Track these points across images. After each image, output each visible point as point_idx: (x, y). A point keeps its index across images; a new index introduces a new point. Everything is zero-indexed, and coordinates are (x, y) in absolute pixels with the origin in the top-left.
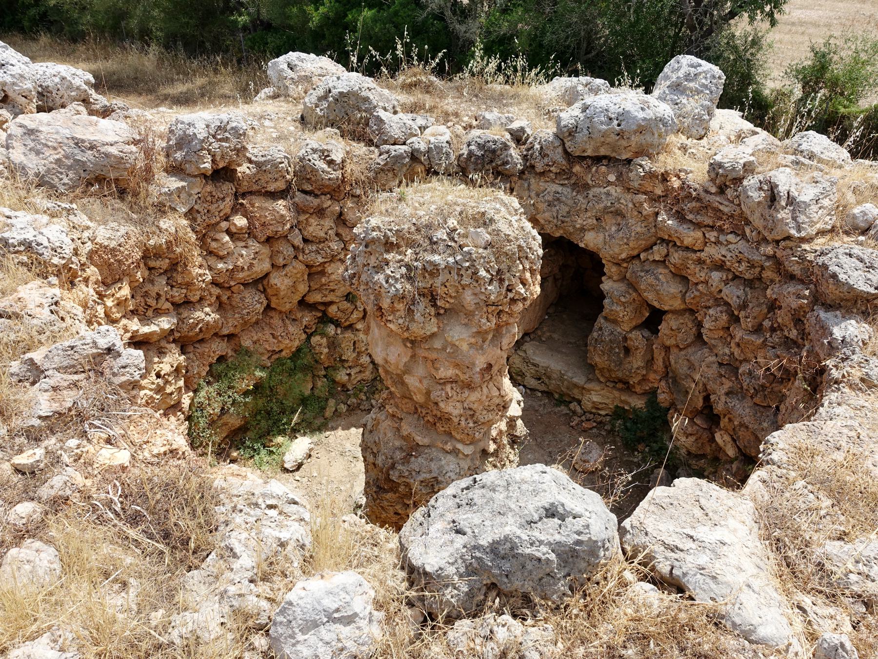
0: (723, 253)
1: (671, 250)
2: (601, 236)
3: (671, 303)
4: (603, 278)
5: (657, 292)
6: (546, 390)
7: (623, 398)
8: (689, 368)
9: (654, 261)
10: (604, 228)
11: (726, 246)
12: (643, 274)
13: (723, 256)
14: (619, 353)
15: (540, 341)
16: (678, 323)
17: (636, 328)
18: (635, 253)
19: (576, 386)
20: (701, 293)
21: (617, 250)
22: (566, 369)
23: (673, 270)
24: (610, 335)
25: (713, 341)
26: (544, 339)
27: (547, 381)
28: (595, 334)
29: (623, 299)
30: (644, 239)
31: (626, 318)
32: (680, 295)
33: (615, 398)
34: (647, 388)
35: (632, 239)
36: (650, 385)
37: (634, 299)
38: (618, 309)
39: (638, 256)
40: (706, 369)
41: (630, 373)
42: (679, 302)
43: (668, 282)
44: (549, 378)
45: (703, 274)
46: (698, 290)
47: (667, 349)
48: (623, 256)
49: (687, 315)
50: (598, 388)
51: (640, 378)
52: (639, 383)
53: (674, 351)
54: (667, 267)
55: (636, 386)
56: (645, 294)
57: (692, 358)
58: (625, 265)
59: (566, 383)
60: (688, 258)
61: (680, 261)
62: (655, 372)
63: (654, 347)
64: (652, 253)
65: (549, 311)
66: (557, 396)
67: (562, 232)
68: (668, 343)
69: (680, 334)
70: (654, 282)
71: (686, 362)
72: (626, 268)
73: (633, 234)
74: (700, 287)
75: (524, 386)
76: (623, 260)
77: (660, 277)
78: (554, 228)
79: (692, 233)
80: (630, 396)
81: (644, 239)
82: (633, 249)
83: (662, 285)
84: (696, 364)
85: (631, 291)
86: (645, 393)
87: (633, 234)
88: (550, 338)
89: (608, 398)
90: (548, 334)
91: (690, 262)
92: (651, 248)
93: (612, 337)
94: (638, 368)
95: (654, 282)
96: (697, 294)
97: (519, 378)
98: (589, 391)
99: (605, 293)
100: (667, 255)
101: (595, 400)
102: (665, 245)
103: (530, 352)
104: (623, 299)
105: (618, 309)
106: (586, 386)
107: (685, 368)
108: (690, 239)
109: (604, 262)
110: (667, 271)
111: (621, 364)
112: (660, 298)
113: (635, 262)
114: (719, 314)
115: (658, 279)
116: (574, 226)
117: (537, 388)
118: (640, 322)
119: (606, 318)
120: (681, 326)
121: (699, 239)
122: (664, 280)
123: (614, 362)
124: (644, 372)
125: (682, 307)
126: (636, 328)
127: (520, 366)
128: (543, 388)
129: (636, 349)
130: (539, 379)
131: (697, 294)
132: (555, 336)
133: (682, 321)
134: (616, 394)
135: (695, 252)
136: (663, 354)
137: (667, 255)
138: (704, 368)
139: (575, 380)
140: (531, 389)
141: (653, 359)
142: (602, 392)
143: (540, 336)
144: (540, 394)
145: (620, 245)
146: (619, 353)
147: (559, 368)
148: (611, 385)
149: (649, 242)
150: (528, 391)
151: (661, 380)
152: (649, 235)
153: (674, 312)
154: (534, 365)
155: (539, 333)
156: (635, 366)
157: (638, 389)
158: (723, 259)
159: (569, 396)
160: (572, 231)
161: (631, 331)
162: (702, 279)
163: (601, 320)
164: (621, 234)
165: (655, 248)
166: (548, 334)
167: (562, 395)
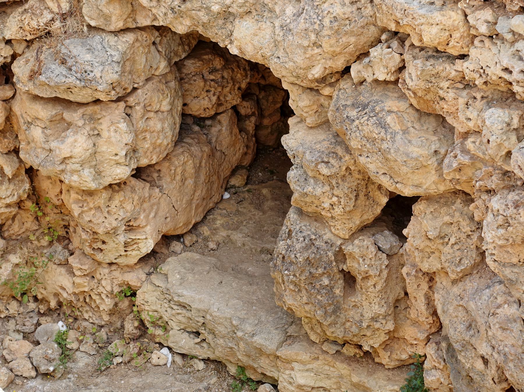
0: (506, 63)
1: (407, 57)
2: (266, 26)
3: (416, 178)
4: (291, 121)
5: (384, 154)
6: (212, 357)
7: (355, 379)
8: (469, 327)
9: (376, 81)
10: (271, 11)
11: (513, 43)
12: (353, 113)
13: (506, 70)
14: (330, 289)
15: (205, 251)
16: (438, 223)
17: (363, 229)
18: (340, 64)
19: (260, 352)
20: (473, 157)
21: (300, 59)
22: (242, 314)
23: (414, 102)
24: (306, 248)
25: (507, 272)
26: (212, 245)
27: (210, 338)
28: (281, 246)
29: (324, 170)
30: (351, 33)
31: (338, 210)
32: (433, 162)
33: (341, 377)
34: (404, 356)
35: (325, 32)
36: (410, 350)
37: (347, 169)
38: (319, 191)
39: (347, 70)
40: (499, 334)
41: (360, 328)
42: (433, 177)
43: (405, 132)
44: (212, 332)
45: (472, 113)
46: (465, 151)
47: (431, 278)
48: (317, 72)
49: (458, 204)
50: (305, 357)
51: (383, 338)
52: (386, 346)
53: (441, 282)
54: (403, 97)
55: (381, 353)
56: (362, 160)
57: (472, 305)
58: (327, 91)
59: (242, 345)
60: (437, 75)
61: (423, 85)
62: (415, 323)
63: (404, 271)
64: (370, 65)
65: (234, 181)
66: (233, 370)
67: (187, 22)
68: (425, 267)
69: (447, 249)
70: (376, 132)
71: (461, 314)
72: (330, 97)
73: (327, 22)
74: (469, 144)
75: (170, 349)
76: (323, 80)
77: (389, 119)
78: (170, 16)
79: (437, 16)
80: (370, 374)
81: (351, 33)
82: (334, 55)
83: (393, 138)
84: (481, 321)
85: (340, 151)
86: (401, 366)
87: (327, 22)
88: (228, 240)
89: (328, 377)
90: (224, 233)
91: (445, 84)
92: (367, 54)
93: (310, 254)
94: (374, 319)
95: (376, 132)
96: (465, 159)
97: (159, 332)
98: (288, 362)
99: (290, 154)
100: (402, 68)
101: (301, 381)
102: (395, 44)
103: (174, 278)
104: (324, 170)
105: (319, 191)
106: (285, 352)
107: (461, 327)
108: (435, 30)
109: (285, 86)
110: (403, 105)
111: (337, 310)
112: (391, 168)
113: (344, 84)
114: (511, 211)
115: (383, 125)
116: (208, 9)
117: (194, 352)
118: (370, 216)
119: (300, 212)
120: (448, 230)
121: (456, 29)
122: (397, 128)
123: (322, 307)
124: (390, 326)
125: (442, 188)
126: (363, 229)
127: (157, 307)
128: (204, 352)
129: (366, 278)
130: (198, 334)
131: (465, 159)
132: (238, 237)
133: (447, 219)
134: (343, 368)
135: (452, 59)
136: (425, 286)
137: (402, 68)
138: (495, 331)
139: (258, 340)
140: (183, 356)
141: (406, 294)
142: (315, 365)
143: (206, 239)
144: (201, 365)
145: (306, 48)
146: (330, 289)
147: (228, 312)
148: (332, 349)
149: (363, 40)
150: (178, 360)
151: (428, 340)
152: (362, 22)
153: (429, 198)
154: (183, 306)
155: (205, 230)
156: (368, 315)
157: (384, 358)
158: (506, 76)
159: (255, 370)
160: (205, 19)
161: (353, 236)
162: (471, 124)
163: (292, 215)
164: (302, 24)
165: (374, 52)
166: (224, 233)
167: (242, 369)
